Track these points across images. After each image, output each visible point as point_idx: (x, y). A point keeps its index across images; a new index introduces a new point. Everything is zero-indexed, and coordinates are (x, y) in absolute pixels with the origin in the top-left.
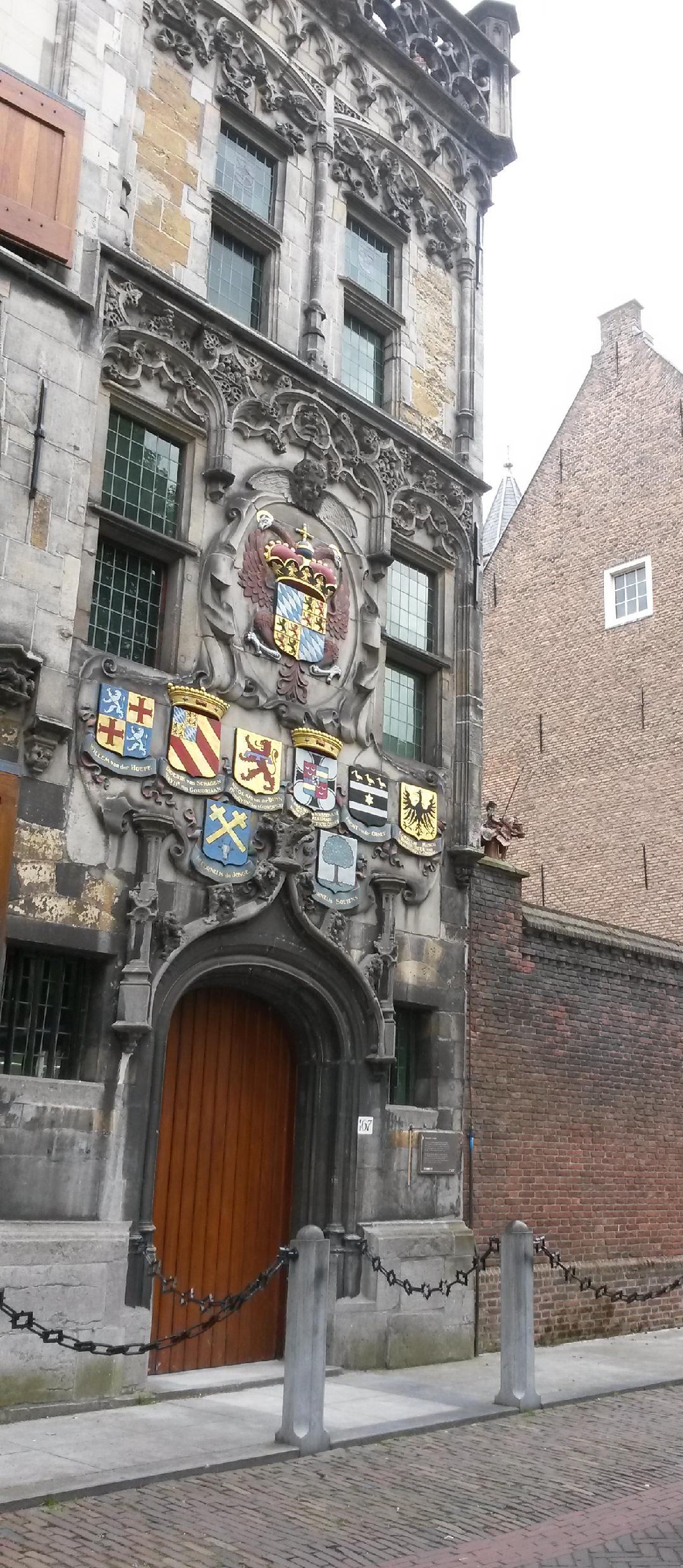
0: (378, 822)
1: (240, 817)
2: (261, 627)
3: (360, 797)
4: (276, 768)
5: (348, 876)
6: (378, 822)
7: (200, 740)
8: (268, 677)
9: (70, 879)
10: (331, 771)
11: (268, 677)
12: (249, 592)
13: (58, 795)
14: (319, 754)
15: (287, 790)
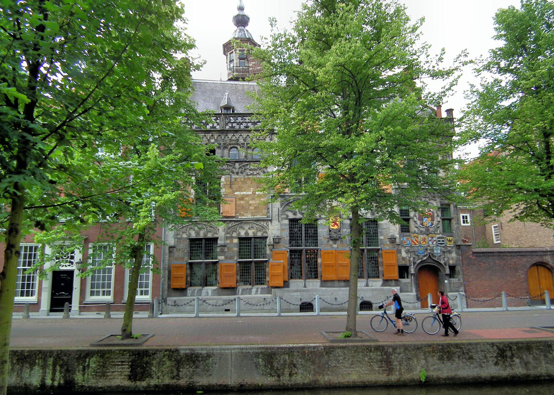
0: (443, 244)
1: (422, 248)
2: (422, 224)
3: (440, 241)
4: (427, 241)
5: (439, 251)
6: (443, 244)
7: (416, 240)
8: (424, 230)
9: (404, 259)
10: (435, 239)
11: (424, 230)
12: (419, 220)
13: (400, 250)
14: (432, 237)
15: (428, 243)
